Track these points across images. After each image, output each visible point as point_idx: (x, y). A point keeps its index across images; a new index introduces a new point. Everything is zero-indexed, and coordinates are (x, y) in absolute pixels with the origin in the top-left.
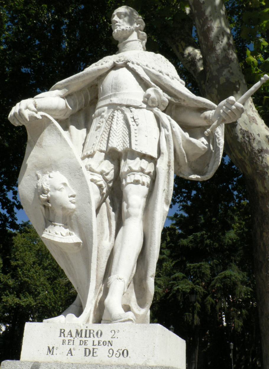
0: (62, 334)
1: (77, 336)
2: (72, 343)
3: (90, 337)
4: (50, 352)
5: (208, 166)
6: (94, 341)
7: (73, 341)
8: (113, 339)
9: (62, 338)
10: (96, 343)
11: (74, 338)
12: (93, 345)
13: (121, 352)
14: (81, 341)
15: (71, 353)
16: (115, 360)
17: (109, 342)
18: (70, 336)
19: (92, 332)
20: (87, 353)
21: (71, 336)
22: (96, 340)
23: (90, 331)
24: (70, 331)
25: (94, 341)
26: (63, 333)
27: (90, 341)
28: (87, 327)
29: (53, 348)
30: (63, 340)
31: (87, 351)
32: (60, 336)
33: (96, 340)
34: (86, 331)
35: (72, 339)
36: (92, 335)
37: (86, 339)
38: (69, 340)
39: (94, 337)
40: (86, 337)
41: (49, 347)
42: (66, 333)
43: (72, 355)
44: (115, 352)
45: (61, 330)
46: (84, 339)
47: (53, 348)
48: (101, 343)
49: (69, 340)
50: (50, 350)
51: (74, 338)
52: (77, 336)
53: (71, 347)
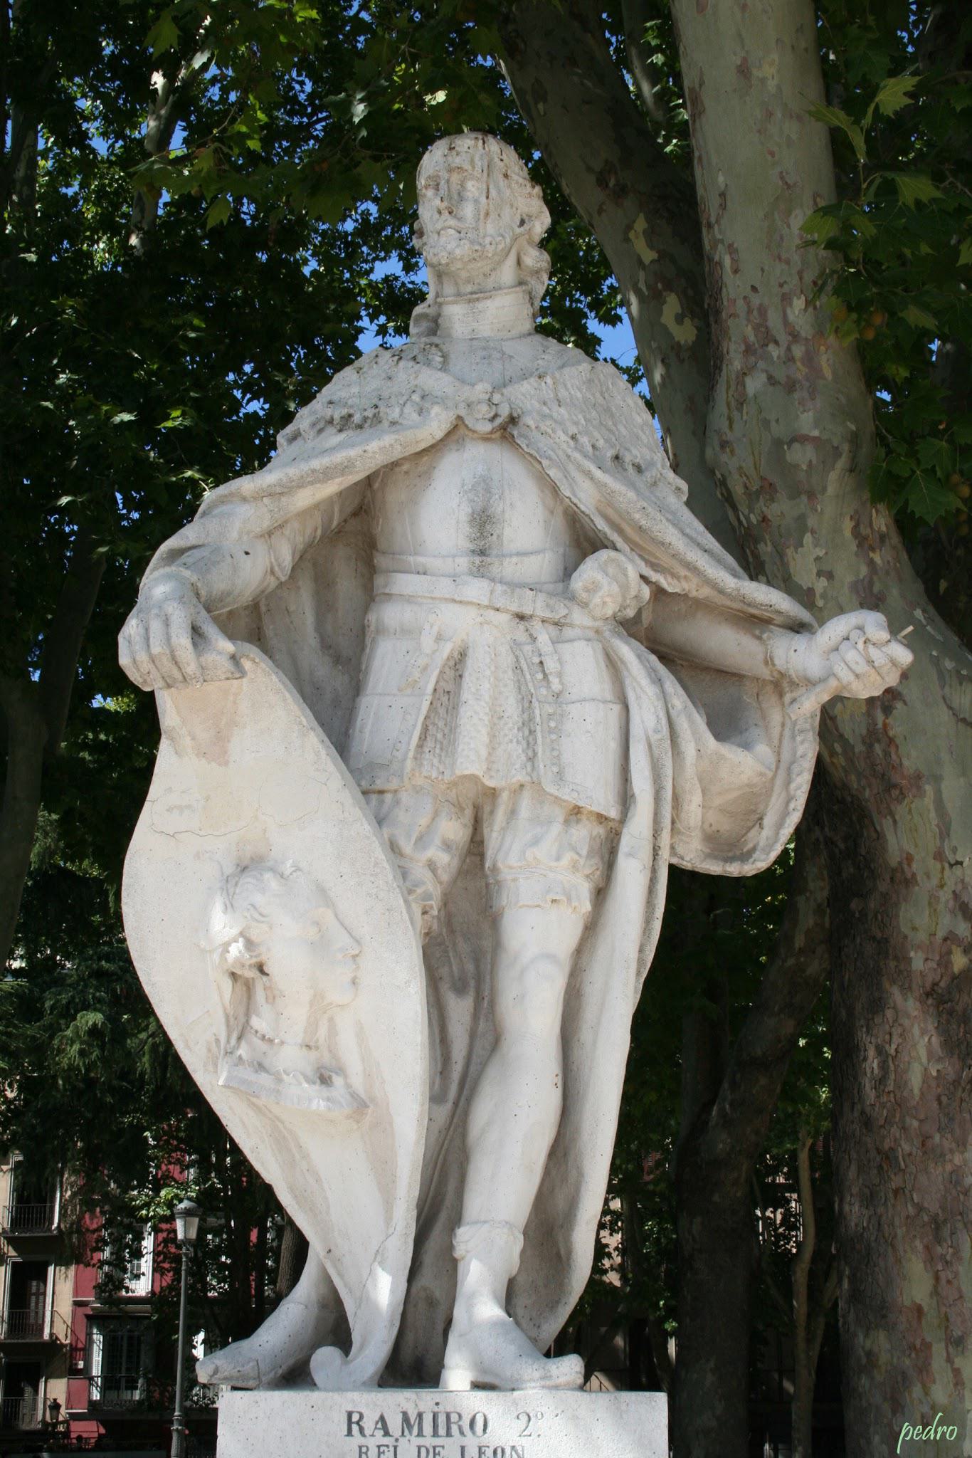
0: (355, 1428)
1: (406, 1432)
3: (449, 1434)
5: (761, 827)
6: (463, 1448)
7: (395, 1447)
8: (524, 1441)
9: (357, 1439)
11: (397, 1440)
14: (419, 1448)
17: (513, 1448)
18: (382, 1432)
19: (454, 1418)
21: (387, 1433)
23: (448, 1416)
25: (463, 1448)
26: (358, 1423)
28: (437, 1404)
30: (360, 1447)
32: (350, 1433)
35: (387, 1440)
36: (454, 1429)
37: (437, 1441)
38: (379, 1447)
39: (462, 1433)
40: (435, 1434)
41: (405, 1414)
42: (368, 1424)
45: (350, 1415)
46: (429, 1441)
49: (379, 1447)
51: (397, 1440)
52: (406, 1432)
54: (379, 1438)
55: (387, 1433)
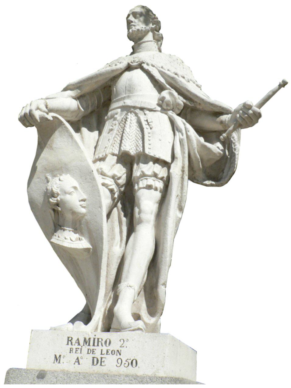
0: (70, 342)
1: (85, 344)
2: (79, 351)
3: (98, 345)
4: (57, 360)
5: (223, 172)
6: (102, 350)
7: (81, 349)
9: (70, 346)
10: (104, 352)
11: (82, 347)
12: (102, 354)
13: (130, 362)
14: (88, 349)
15: (78, 362)
16: (123, 370)
17: (118, 351)
18: (77, 344)
19: (100, 340)
20: (95, 362)
21: (79, 344)
22: (105, 349)
23: (98, 339)
24: (78, 339)
25: (102, 350)
26: (70, 341)
27: (98, 350)
28: (95, 335)
29: (60, 356)
30: (71, 349)
31: (95, 360)
32: (68, 344)
33: (105, 349)
34: (94, 339)
35: (80, 347)
36: (100, 344)
38: (76, 349)
39: (102, 345)
40: (94, 345)
41: (55, 355)
42: (74, 341)
43: (79, 364)
44: (124, 362)
45: (68, 338)
46: (92, 347)
47: (60, 356)
48: (110, 352)
49: (76, 349)
50: (57, 359)
51: (82, 347)
52: (85, 344)
53: (79, 355)
54: (77, 346)
55: (79, 344)
